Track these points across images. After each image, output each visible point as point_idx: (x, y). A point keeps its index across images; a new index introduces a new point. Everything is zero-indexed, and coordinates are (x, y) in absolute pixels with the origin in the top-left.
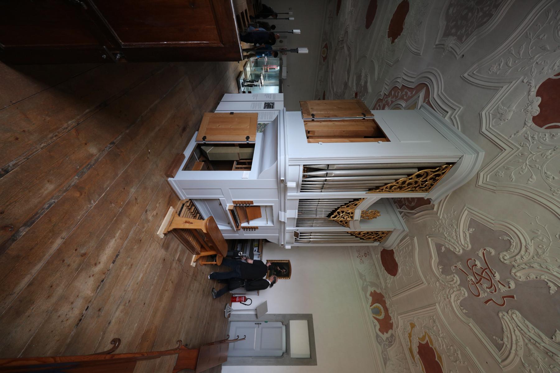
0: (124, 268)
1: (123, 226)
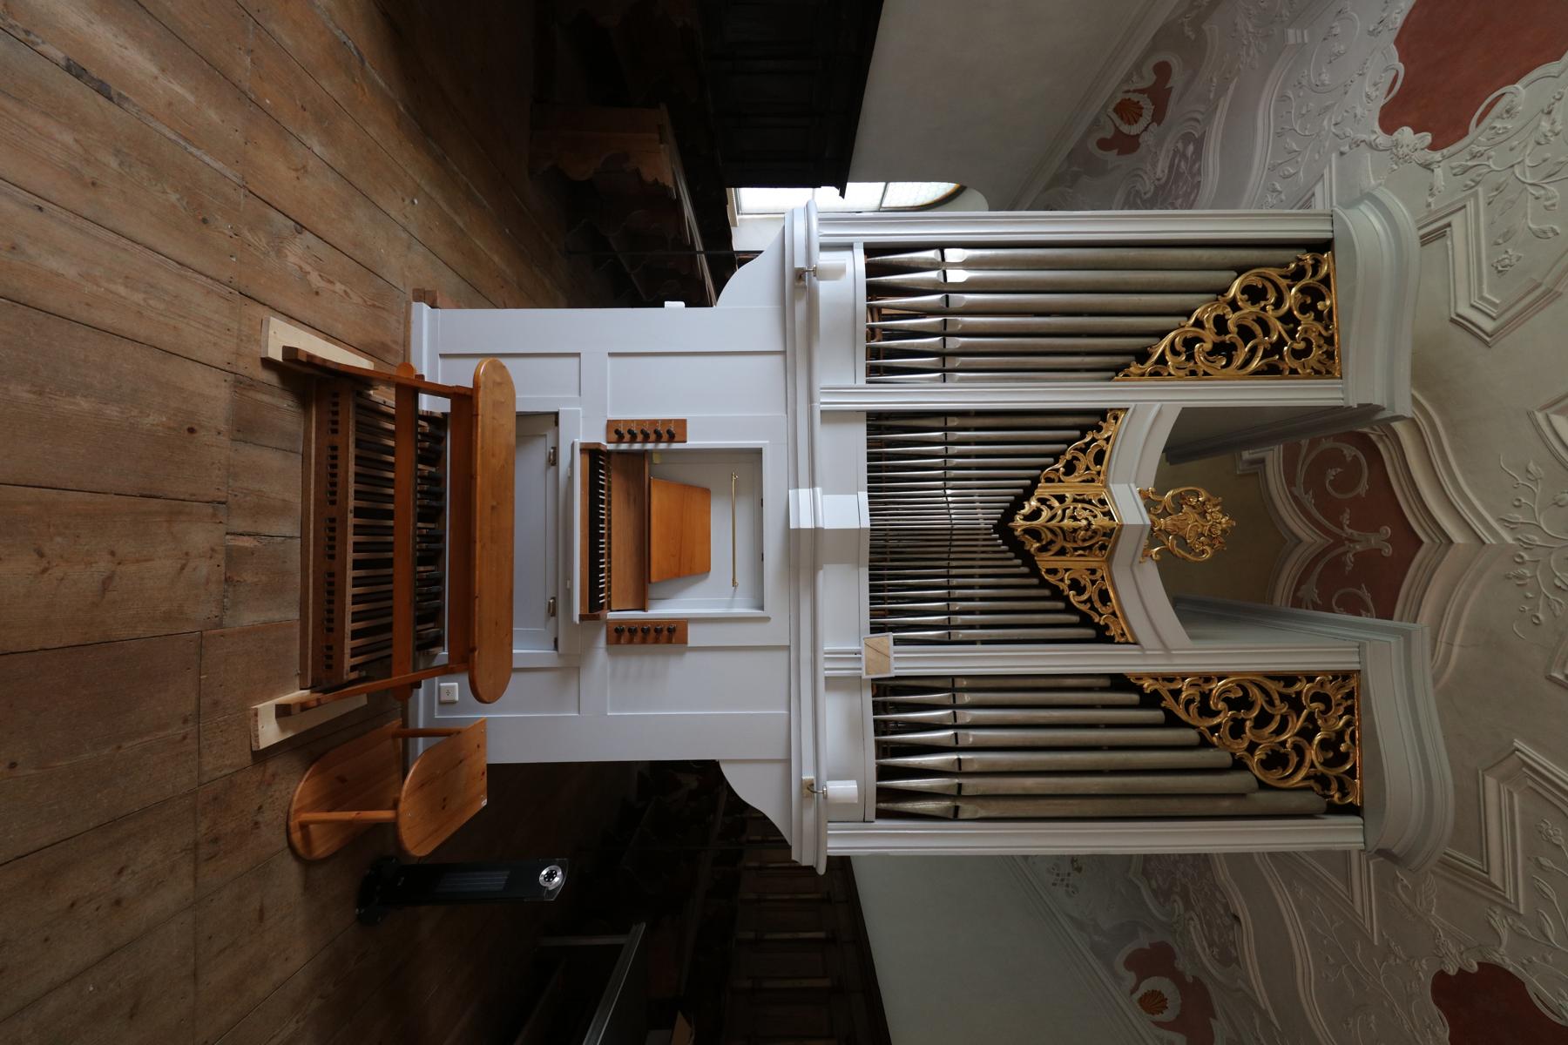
0: (67, 138)
1: (213, 115)
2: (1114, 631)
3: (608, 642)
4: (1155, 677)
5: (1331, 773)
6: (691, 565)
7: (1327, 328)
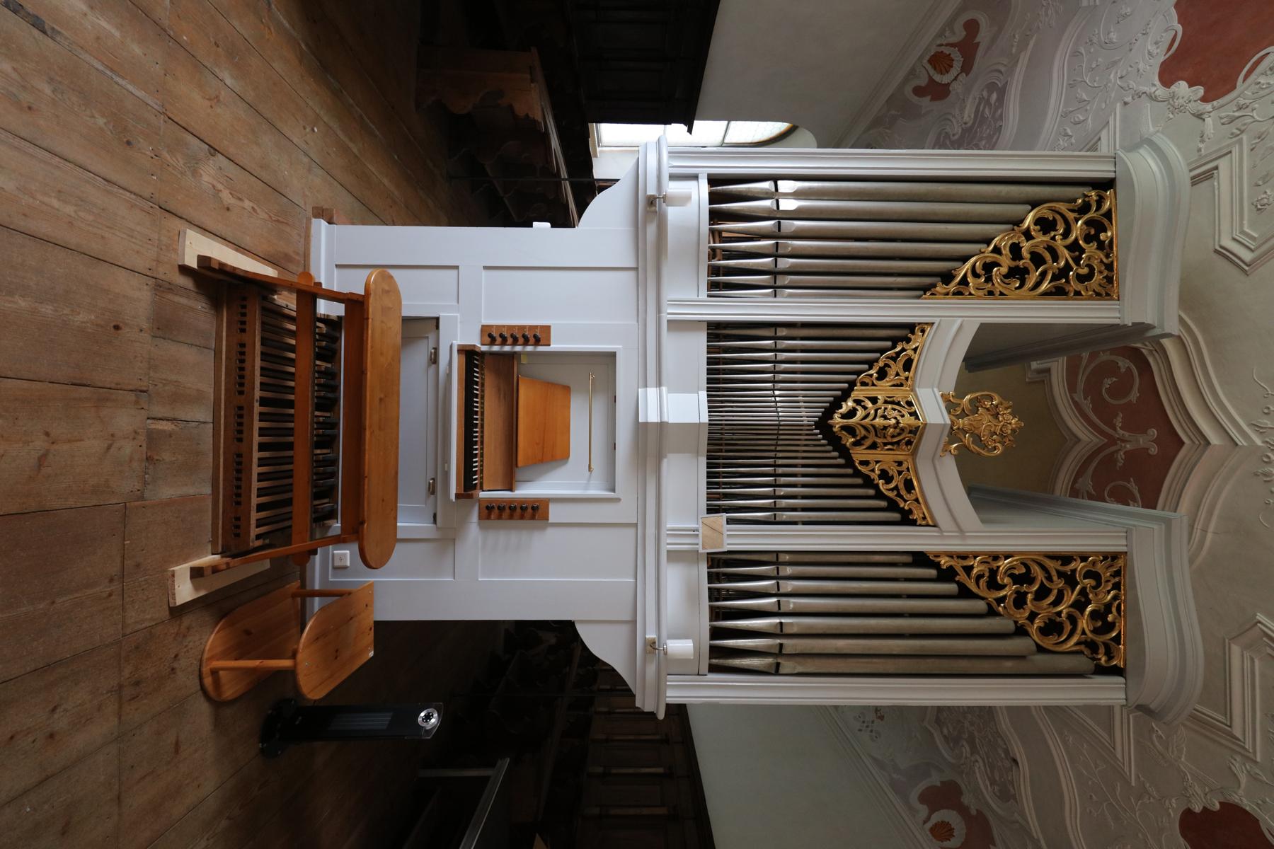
1: (137, 50)
2: (916, 515)
3: (480, 518)
4: (951, 555)
5: (1099, 639)
6: (553, 453)
7: (1107, 256)
